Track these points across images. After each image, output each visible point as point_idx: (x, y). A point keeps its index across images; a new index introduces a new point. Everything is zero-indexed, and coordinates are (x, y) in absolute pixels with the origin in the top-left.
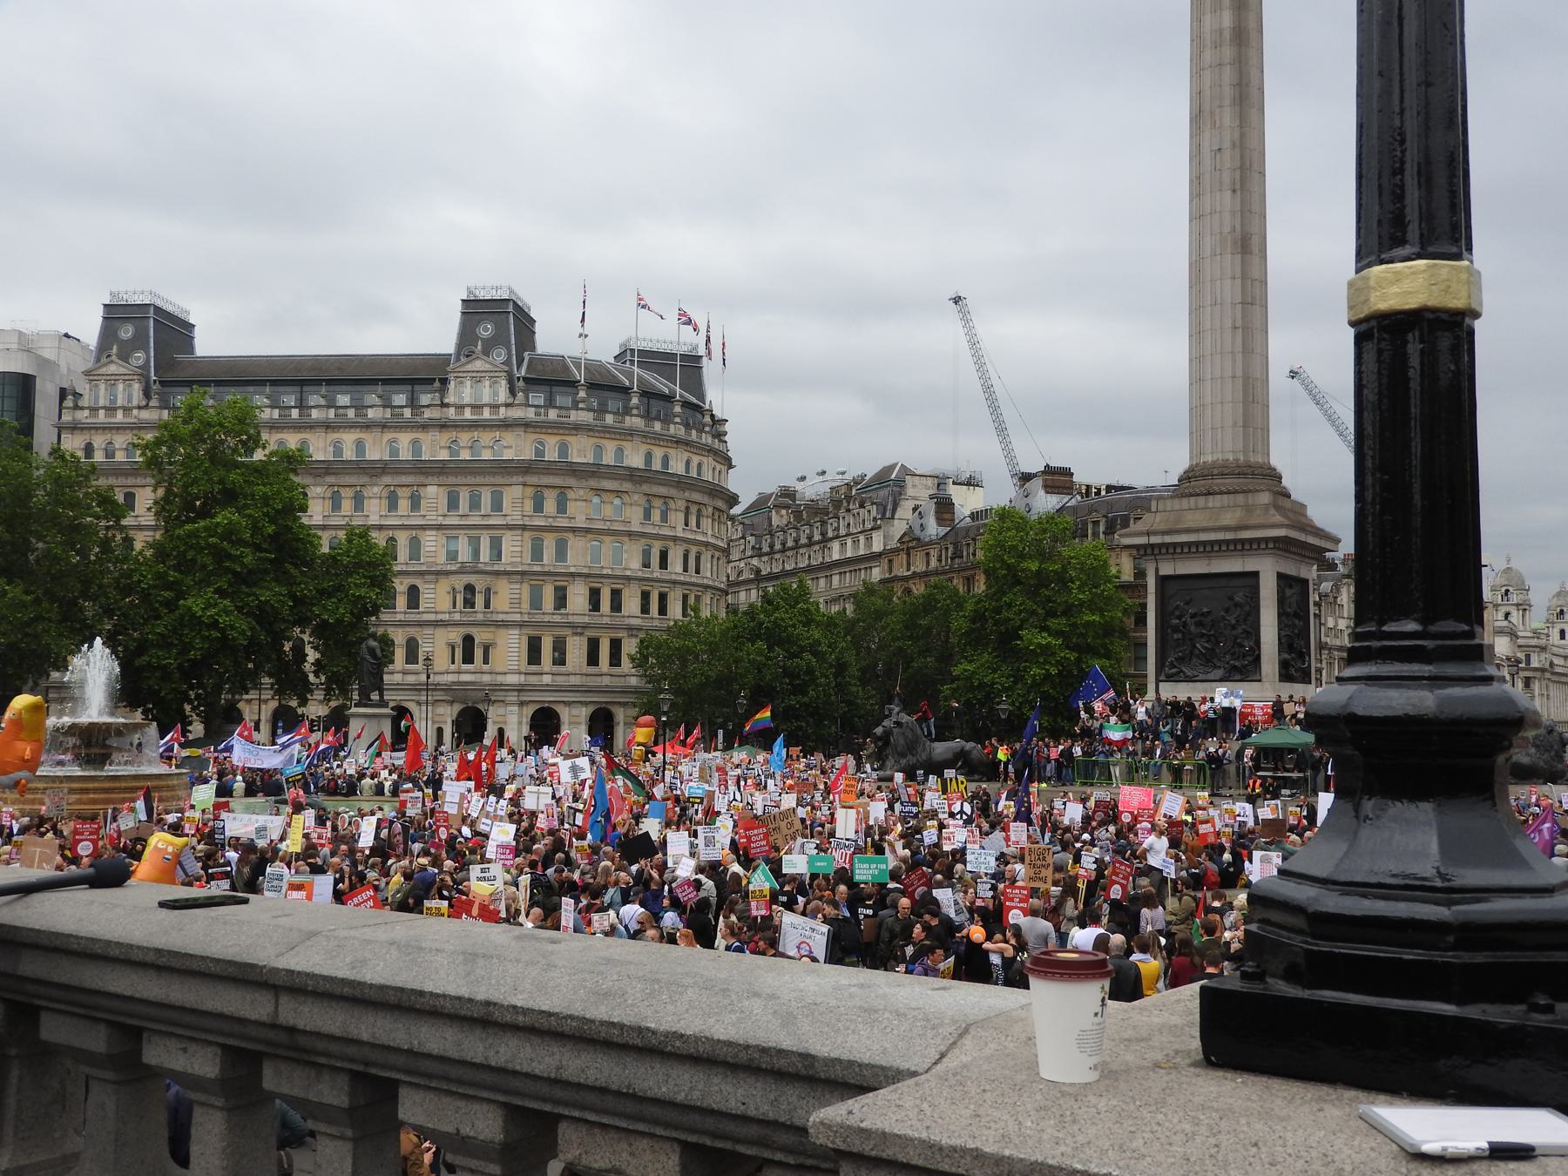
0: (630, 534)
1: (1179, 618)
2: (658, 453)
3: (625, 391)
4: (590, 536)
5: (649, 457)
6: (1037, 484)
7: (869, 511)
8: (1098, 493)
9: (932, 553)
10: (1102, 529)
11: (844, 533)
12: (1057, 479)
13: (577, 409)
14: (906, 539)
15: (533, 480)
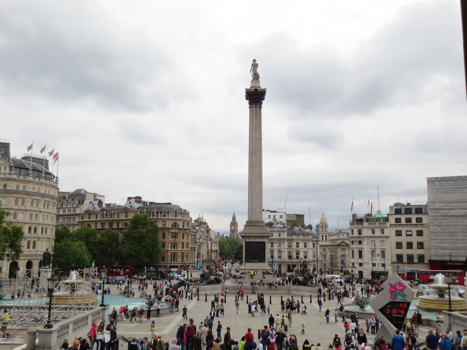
0: (40, 212)
1: (249, 250)
2: (48, 189)
3: (40, 171)
4: (30, 212)
5: (46, 190)
6: (133, 201)
7: (75, 202)
8: (147, 204)
9: (98, 215)
10: (155, 214)
11: (65, 207)
12: (138, 199)
13: (29, 176)
14: (89, 211)
15: (15, 195)
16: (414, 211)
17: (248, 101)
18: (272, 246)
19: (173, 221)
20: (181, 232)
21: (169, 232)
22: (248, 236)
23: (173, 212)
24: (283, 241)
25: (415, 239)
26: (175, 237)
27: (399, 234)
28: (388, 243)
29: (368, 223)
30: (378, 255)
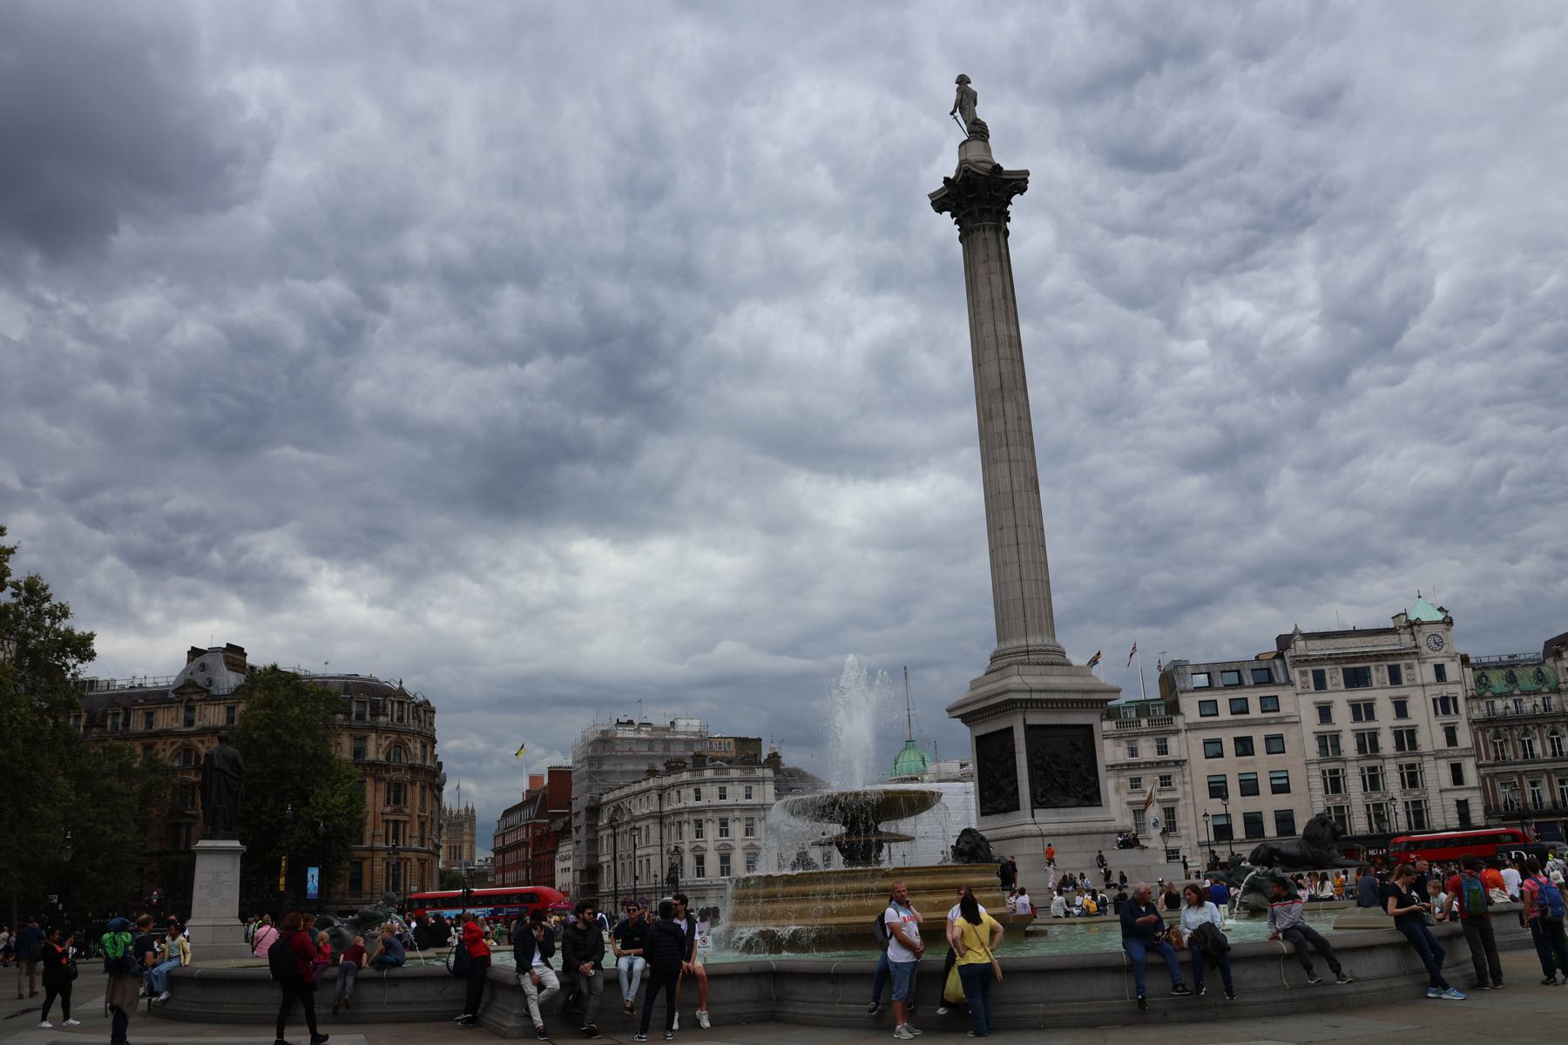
12: (233, 655)
16: (1248, 679)
17: (947, 214)
18: (724, 831)
19: (394, 736)
20: (418, 784)
21: (377, 780)
22: (1037, 701)
23: (393, 702)
24: (762, 813)
25: (1262, 764)
26: (397, 801)
27: (1213, 749)
28: (1184, 783)
29: (1114, 722)
30: (1154, 824)
